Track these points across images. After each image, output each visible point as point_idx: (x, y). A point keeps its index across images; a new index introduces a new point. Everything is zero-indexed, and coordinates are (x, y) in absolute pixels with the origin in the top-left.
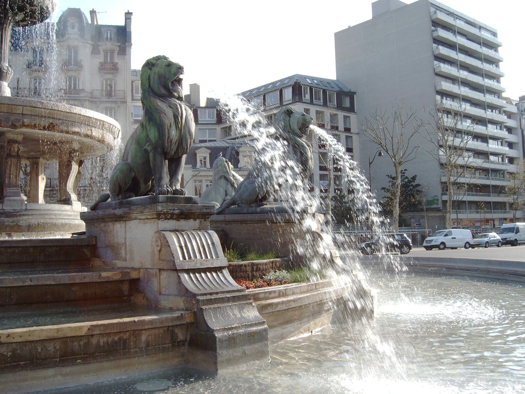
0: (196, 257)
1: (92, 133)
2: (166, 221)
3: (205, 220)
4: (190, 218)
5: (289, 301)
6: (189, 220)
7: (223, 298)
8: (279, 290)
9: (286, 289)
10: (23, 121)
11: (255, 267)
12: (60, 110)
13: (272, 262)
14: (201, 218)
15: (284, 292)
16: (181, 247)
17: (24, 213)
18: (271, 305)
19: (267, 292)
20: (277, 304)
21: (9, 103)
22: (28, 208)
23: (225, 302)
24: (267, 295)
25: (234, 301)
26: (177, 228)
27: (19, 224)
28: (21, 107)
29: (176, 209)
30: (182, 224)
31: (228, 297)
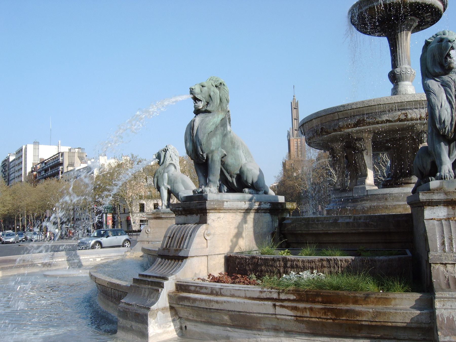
0: (173, 247)
1: (406, 116)
2: (179, 216)
3: (204, 215)
4: (193, 214)
5: (211, 301)
6: (193, 215)
7: (145, 281)
8: (212, 288)
9: (220, 288)
10: (339, 124)
11: (289, 264)
12: (358, 107)
13: (328, 261)
14: (201, 213)
15: (218, 290)
16: (170, 237)
17: (365, 198)
18: (188, 299)
19: (198, 286)
20: (195, 300)
21: (324, 114)
22: (369, 194)
23: (147, 285)
24: (198, 289)
25: (151, 286)
26: (185, 222)
27: (357, 208)
28: (336, 114)
29: (180, 207)
30: (189, 217)
31: (148, 281)
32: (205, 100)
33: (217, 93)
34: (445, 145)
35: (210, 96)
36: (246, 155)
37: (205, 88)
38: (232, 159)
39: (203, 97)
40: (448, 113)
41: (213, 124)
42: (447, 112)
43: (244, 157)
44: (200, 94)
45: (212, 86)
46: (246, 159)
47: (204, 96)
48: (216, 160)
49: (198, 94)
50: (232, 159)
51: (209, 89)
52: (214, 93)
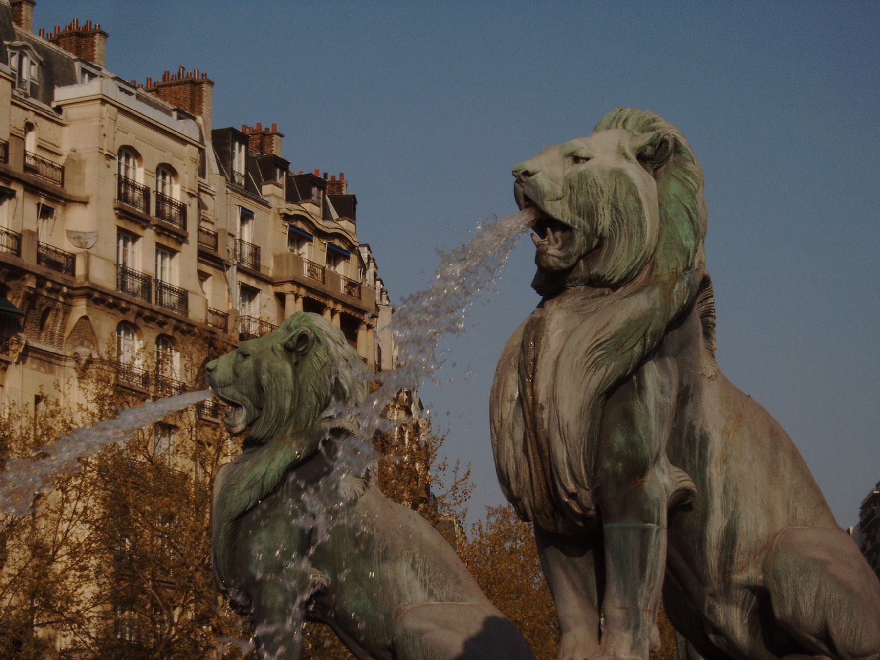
32: (249, 403)
33: (284, 375)
34: (567, 554)
35: (259, 387)
36: (427, 578)
37: (249, 363)
38: (358, 597)
39: (242, 393)
40: (514, 445)
41: (250, 487)
42: (513, 440)
43: (417, 584)
44: (234, 381)
45: (271, 354)
46: (431, 594)
47: (245, 391)
48: (269, 605)
49: (226, 385)
50: (358, 597)
51: (258, 362)
52: (271, 375)
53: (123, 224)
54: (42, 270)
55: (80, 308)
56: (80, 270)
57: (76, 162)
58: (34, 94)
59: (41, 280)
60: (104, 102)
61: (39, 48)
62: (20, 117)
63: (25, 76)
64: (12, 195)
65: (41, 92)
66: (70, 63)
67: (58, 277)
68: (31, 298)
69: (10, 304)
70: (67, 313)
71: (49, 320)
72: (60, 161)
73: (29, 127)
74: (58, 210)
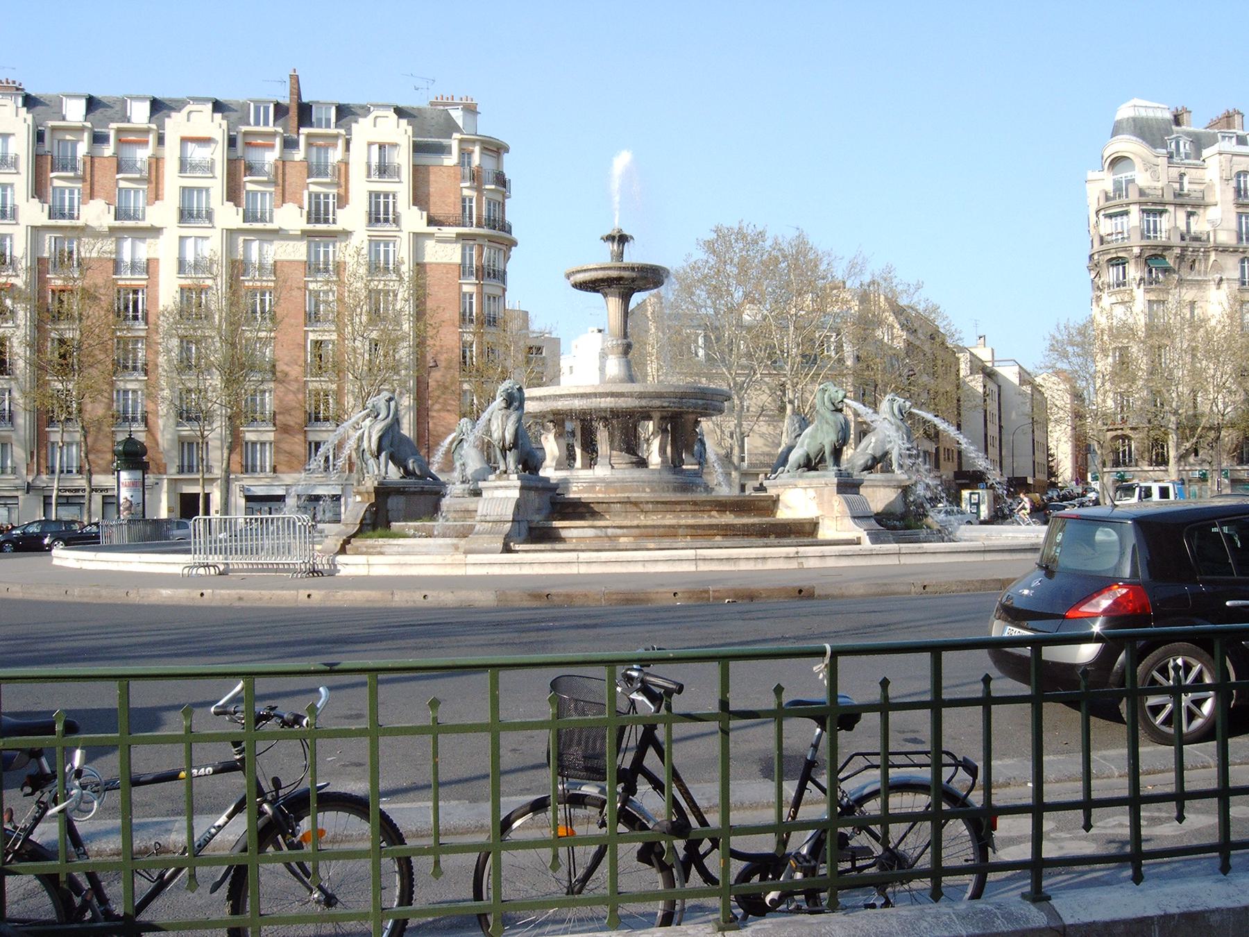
53: (1240, 210)
54: (1184, 244)
55: (1213, 256)
56: (1212, 239)
57: (1211, 187)
58: (1187, 156)
59: (1184, 249)
60: (1221, 154)
61: (1188, 134)
62: (1174, 172)
63: (1182, 149)
64: (1166, 211)
65: (1192, 155)
66: (1215, 134)
67: (1196, 244)
68: (1181, 258)
69: (1167, 263)
70: (1207, 258)
71: (1197, 265)
72: (1202, 187)
73: (1182, 176)
74: (1201, 211)
